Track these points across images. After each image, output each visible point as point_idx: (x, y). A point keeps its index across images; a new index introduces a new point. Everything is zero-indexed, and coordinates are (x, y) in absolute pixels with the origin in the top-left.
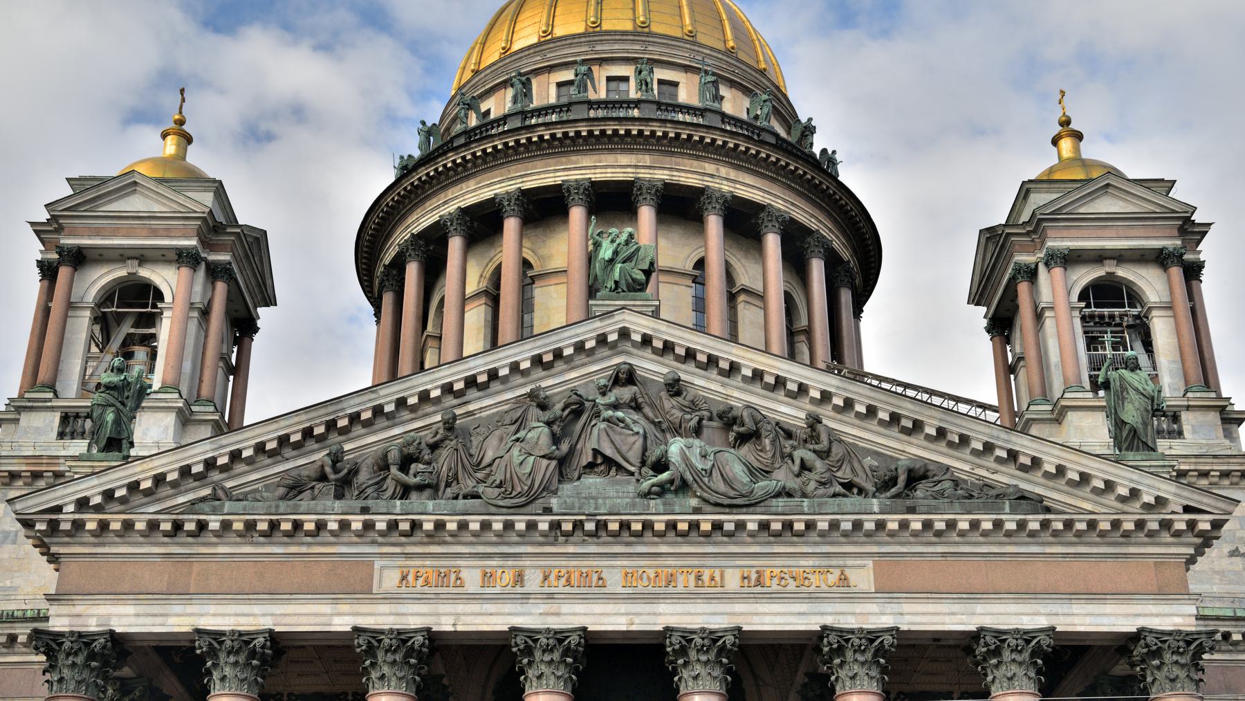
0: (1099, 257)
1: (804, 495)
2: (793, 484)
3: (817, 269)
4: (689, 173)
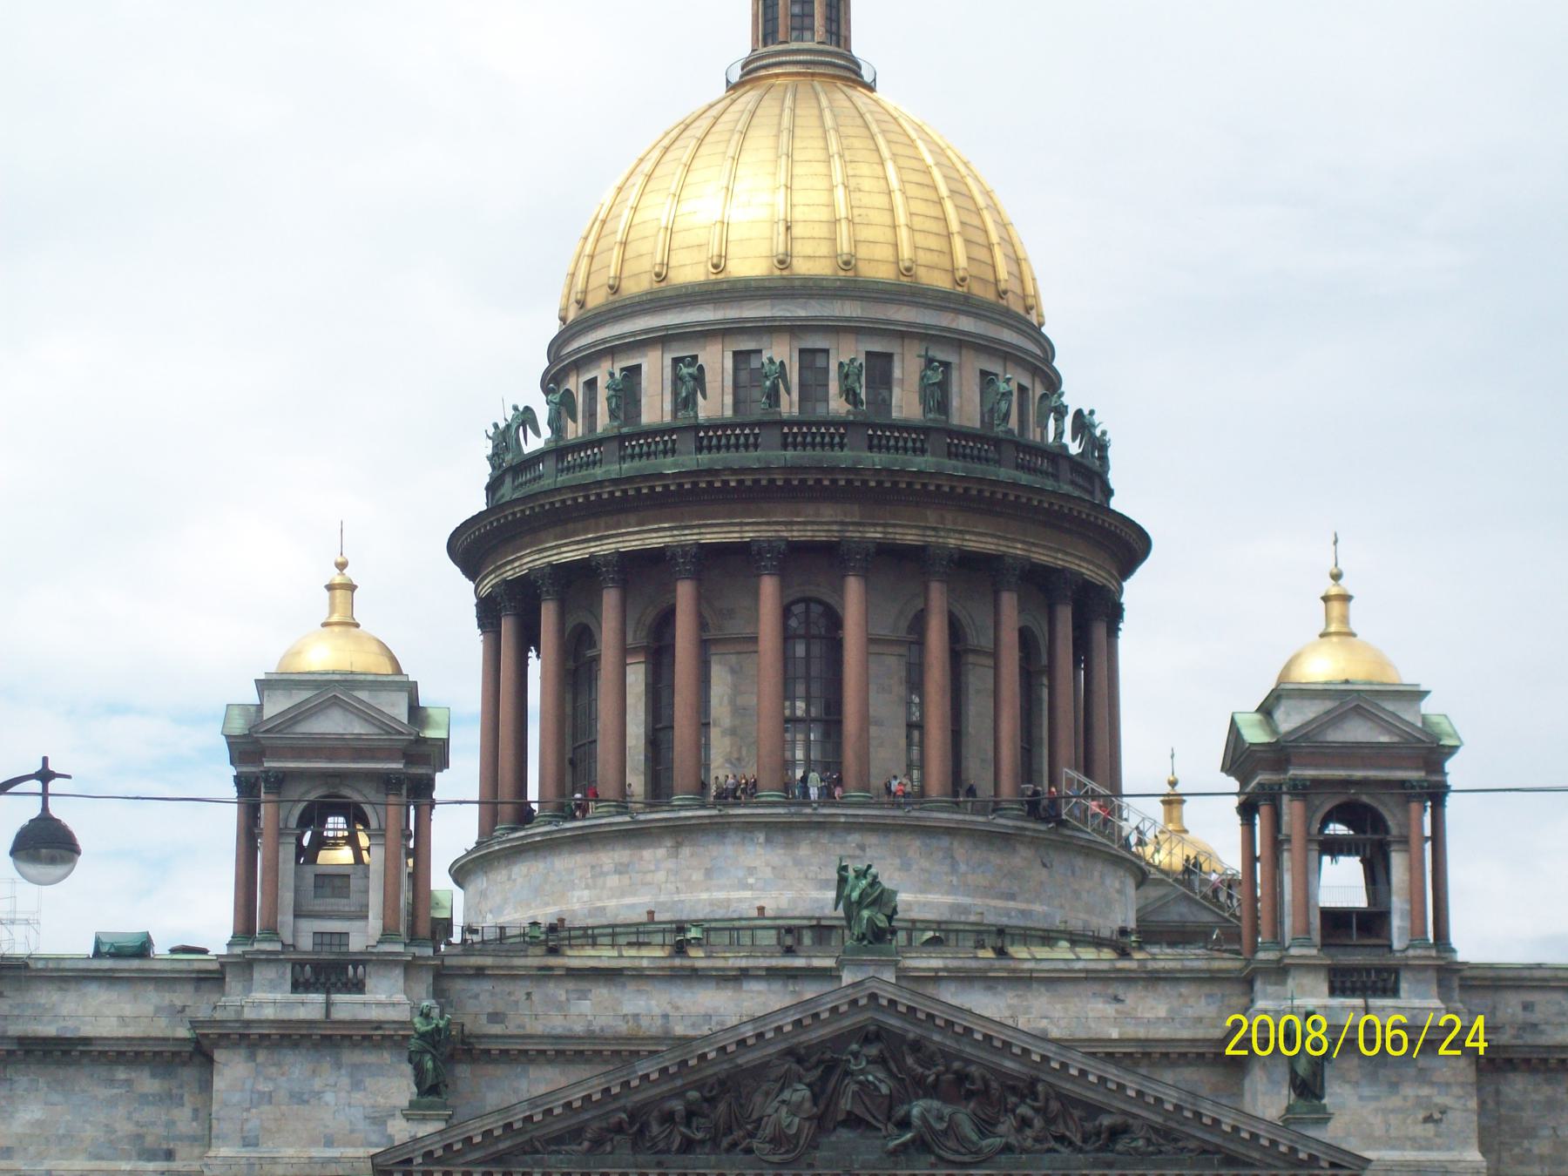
0: (1346, 783)
1: (1024, 1151)
2: (1012, 1140)
3: (1065, 616)
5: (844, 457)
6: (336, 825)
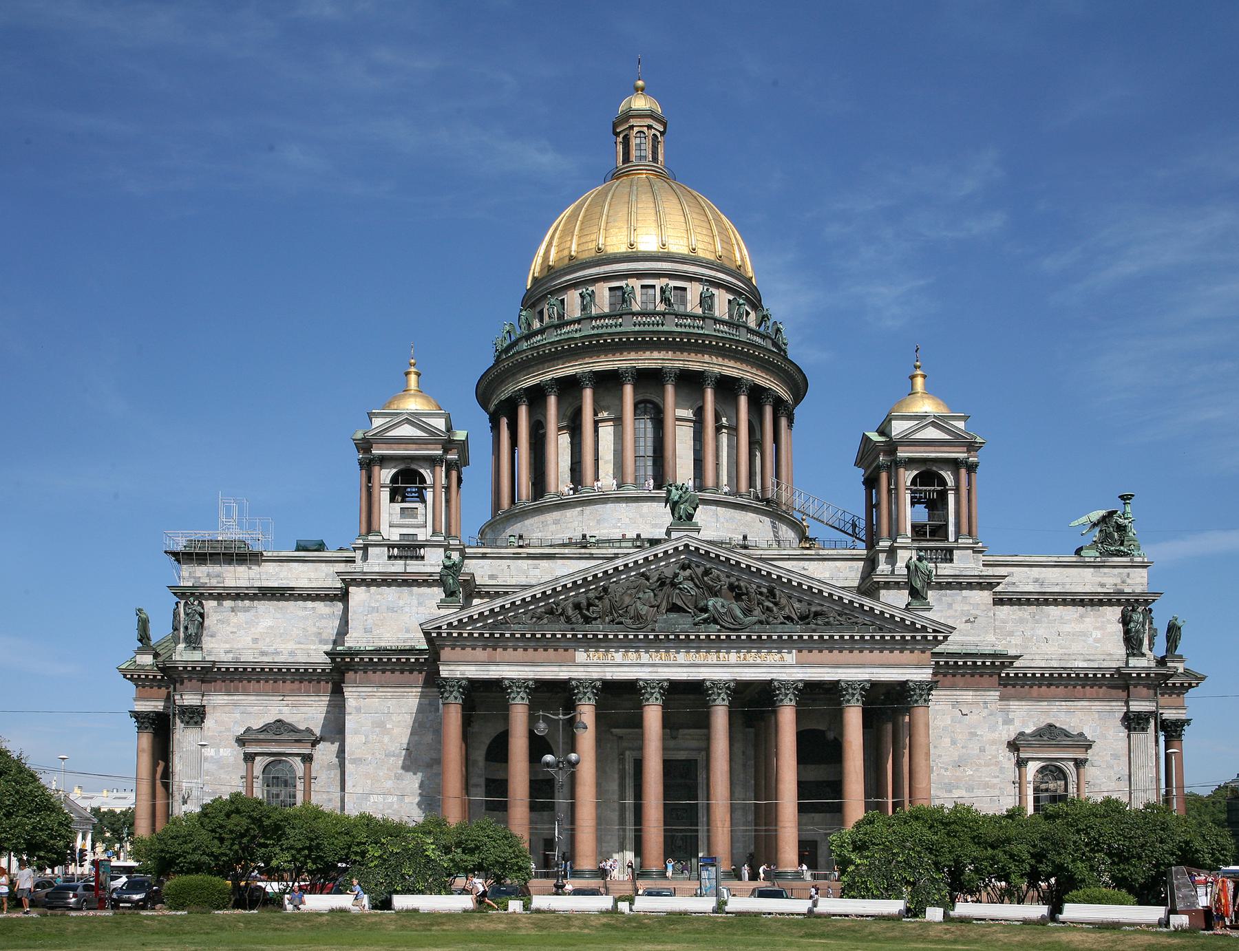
2: (763, 618)
3: (768, 411)
4: (695, 362)
5: (665, 328)
6: (412, 488)
